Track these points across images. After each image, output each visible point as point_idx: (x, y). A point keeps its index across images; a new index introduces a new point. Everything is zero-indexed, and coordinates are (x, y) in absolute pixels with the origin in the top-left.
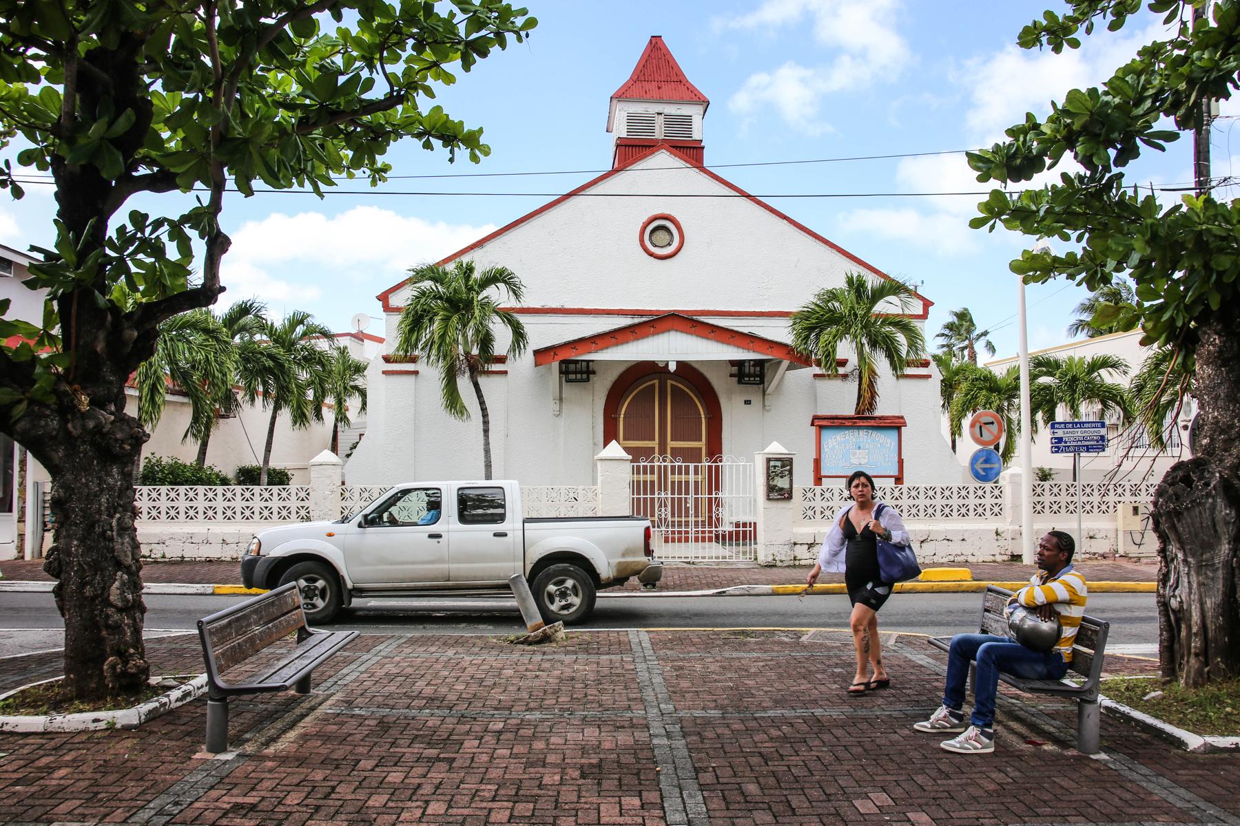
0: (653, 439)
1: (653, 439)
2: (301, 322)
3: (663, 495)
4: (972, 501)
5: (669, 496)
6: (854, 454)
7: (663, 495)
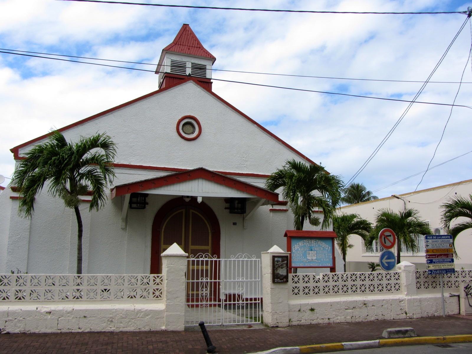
0: (208, 245)
1: (208, 245)
2: (105, 145)
3: (204, 280)
4: (367, 283)
5: (209, 280)
6: (309, 254)
7: (204, 280)
